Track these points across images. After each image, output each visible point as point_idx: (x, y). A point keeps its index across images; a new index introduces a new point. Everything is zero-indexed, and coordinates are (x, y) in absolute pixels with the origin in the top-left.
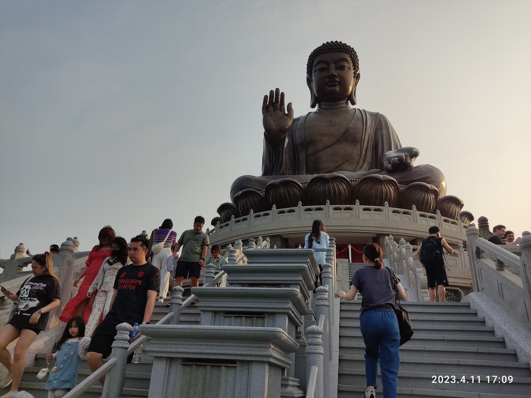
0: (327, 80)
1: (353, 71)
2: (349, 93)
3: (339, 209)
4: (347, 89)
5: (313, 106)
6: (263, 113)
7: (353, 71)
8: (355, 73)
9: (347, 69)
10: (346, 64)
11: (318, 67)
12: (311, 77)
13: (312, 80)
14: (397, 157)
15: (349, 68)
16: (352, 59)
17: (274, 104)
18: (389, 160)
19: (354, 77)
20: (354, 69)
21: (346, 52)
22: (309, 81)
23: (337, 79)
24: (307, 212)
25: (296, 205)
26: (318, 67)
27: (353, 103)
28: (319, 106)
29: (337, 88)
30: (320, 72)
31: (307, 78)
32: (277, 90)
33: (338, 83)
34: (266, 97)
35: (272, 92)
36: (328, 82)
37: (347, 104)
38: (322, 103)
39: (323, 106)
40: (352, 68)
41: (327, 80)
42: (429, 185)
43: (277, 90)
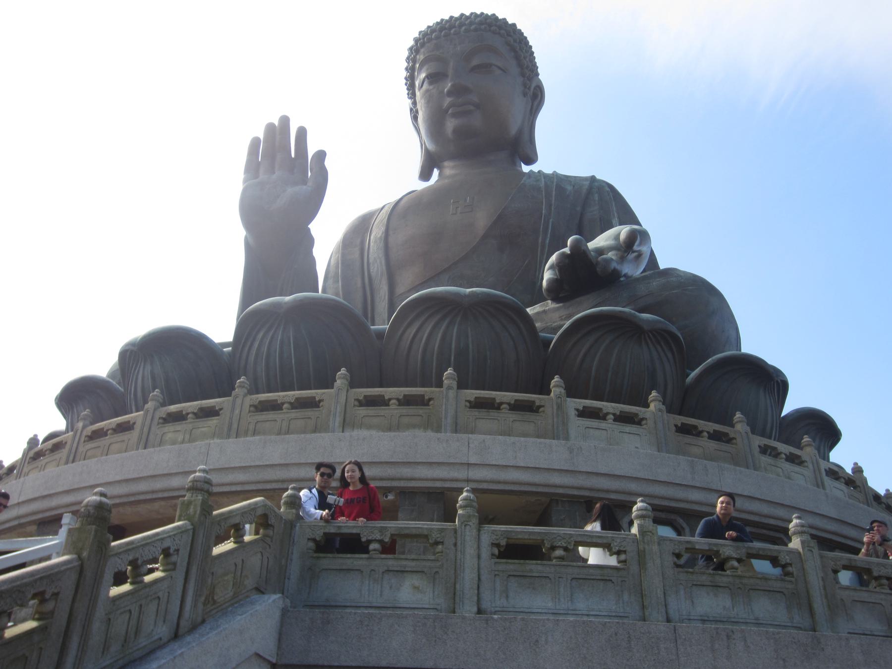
2: (513, 130)
3: (275, 406)
5: (425, 175)
6: (245, 181)
8: (525, 85)
9: (498, 72)
13: (417, 112)
16: (513, 49)
19: (525, 95)
20: (523, 75)
21: (494, 33)
22: (415, 118)
24: (170, 428)
26: (423, 75)
27: (531, 159)
28: (440, 175)
29: (477, 121)
30: (430, 83)
31: (411, 110)
32: (285, 121)
33: (477, 106)
34: (255, 143)
35: (270, 128)
36: (451, 105)
37: (514, 164)
38: (446, 164)
39: (448, 172)
41: (448, 101)
43: (285, 121)
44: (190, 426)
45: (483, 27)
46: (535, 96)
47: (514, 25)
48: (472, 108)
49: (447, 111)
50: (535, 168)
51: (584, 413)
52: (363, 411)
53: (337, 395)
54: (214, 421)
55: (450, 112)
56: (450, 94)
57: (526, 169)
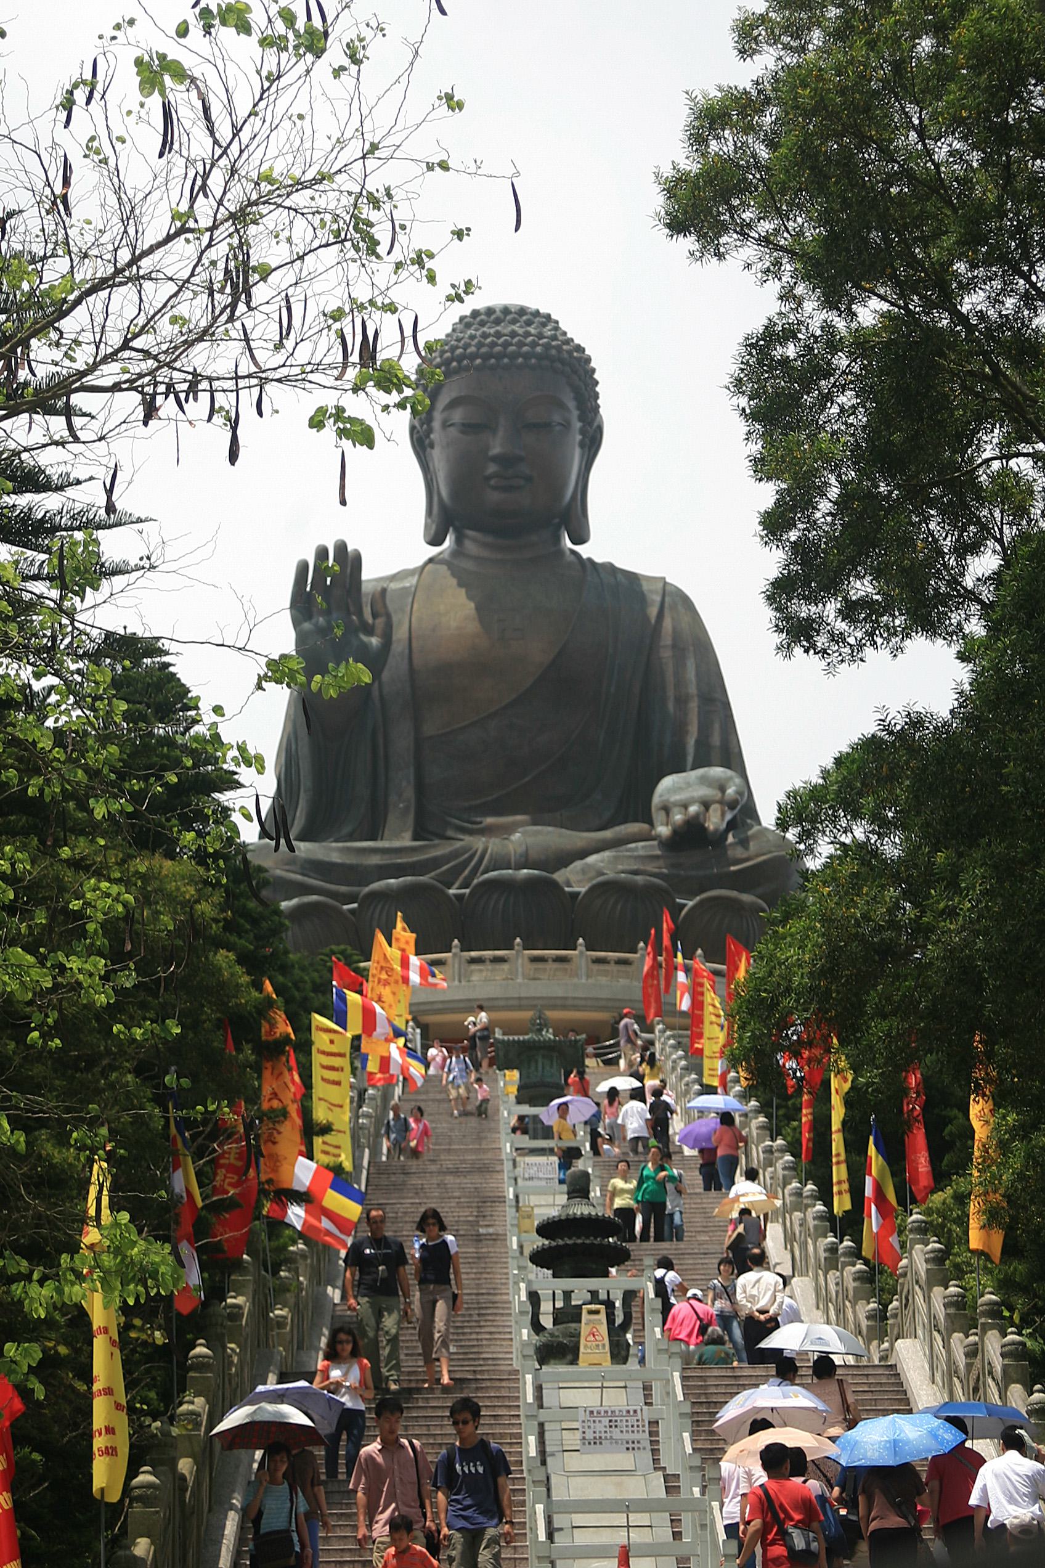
0: (492, 468)
1: (579, 425)
4: (557, 490)
5: (435, 540)
7: (579, 425)
8: (582, 432)
9: (558, 428)
10: (557, 418)
11: (457, 416)
12: (430, 431)
13: (432, 446)
15: (566, 426)
18: (666, 809)
19: (582, 445)
24: (474, 967)
26: (457, 416)
27: (581, 537)
33: (529, 479)
34: (303, 568)
35: (322, 553)
36: (495, 475)
37: (558, 540)
39: (470, 546)
41: (492, 468)
42: (746, 898)
44: (490, 967)
45: (545, 363)
46: (592, 441)
47: (580, 349)
48: (522, 482)
49: (488, 478)
50: (584, 551)
52: (596, 967)
54: (505, 967)
55: (492, 482)
56: (495, 459)
57: (569, 544)
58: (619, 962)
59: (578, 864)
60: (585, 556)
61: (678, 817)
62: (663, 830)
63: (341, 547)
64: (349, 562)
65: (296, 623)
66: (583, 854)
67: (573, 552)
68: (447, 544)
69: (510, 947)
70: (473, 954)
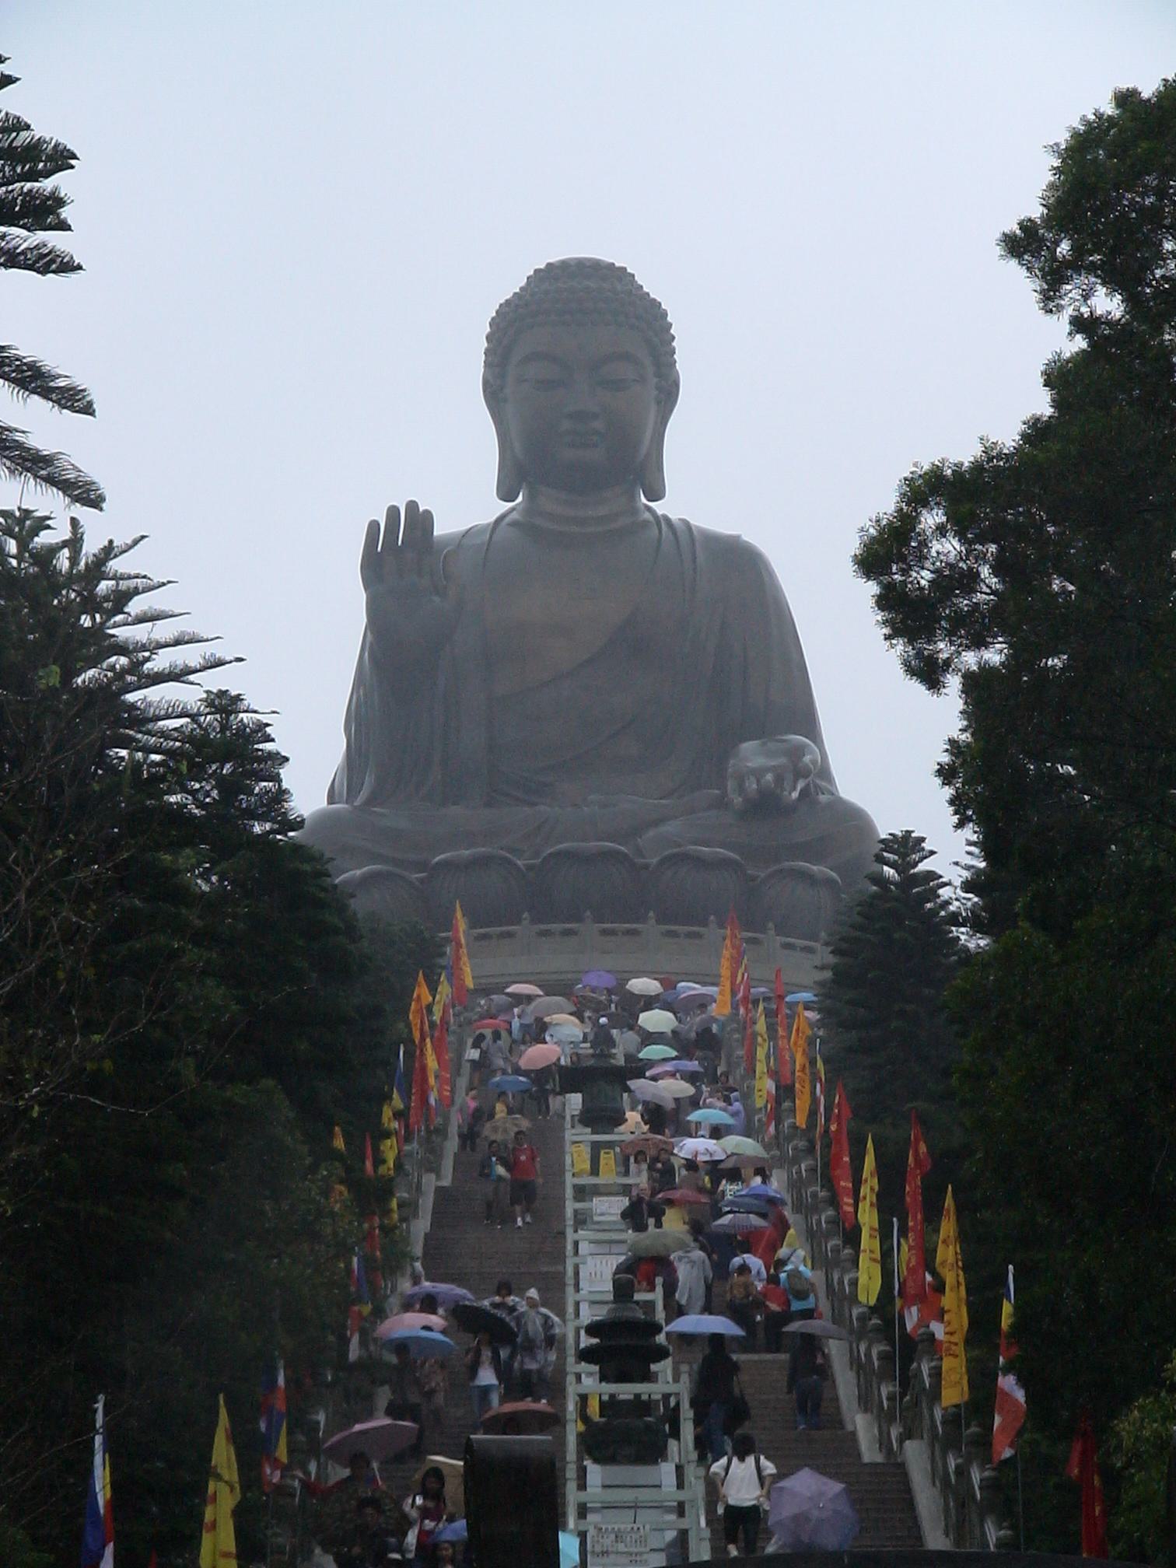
0: (566, 425)
3: (612, 933)
5: (506, 494)
8: (659, 388)
14: (759, 773)
17: (400, 554)
19: (658, 403)
22: (494, 394)
23: (598, 425)
25: (519, 922)
27: (656, 494)
28: (531, 498)
31: (486, 384)
34: (374, 526)
35: (393, 512)
37: (633, 497)
40: (650, 370)
41: (566, 425)
43: (412, 506)
46: (668, 394)
51: (788, 946)
53: (651, 928)
57: (643, 500)
58: (689, 935)
59: (651, 833)
60: (660, 512)
61: (752, 785)
62: (738, 800)
63: (412, 506)
64: (420, 521)
65: (367, 584)
66: (656, 823)
67: (649, 509)
68: (520, 499)
69: (579, 919)
70: (543, 927)
